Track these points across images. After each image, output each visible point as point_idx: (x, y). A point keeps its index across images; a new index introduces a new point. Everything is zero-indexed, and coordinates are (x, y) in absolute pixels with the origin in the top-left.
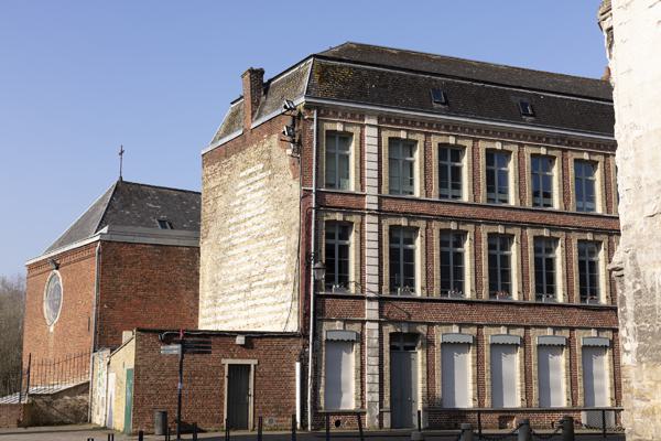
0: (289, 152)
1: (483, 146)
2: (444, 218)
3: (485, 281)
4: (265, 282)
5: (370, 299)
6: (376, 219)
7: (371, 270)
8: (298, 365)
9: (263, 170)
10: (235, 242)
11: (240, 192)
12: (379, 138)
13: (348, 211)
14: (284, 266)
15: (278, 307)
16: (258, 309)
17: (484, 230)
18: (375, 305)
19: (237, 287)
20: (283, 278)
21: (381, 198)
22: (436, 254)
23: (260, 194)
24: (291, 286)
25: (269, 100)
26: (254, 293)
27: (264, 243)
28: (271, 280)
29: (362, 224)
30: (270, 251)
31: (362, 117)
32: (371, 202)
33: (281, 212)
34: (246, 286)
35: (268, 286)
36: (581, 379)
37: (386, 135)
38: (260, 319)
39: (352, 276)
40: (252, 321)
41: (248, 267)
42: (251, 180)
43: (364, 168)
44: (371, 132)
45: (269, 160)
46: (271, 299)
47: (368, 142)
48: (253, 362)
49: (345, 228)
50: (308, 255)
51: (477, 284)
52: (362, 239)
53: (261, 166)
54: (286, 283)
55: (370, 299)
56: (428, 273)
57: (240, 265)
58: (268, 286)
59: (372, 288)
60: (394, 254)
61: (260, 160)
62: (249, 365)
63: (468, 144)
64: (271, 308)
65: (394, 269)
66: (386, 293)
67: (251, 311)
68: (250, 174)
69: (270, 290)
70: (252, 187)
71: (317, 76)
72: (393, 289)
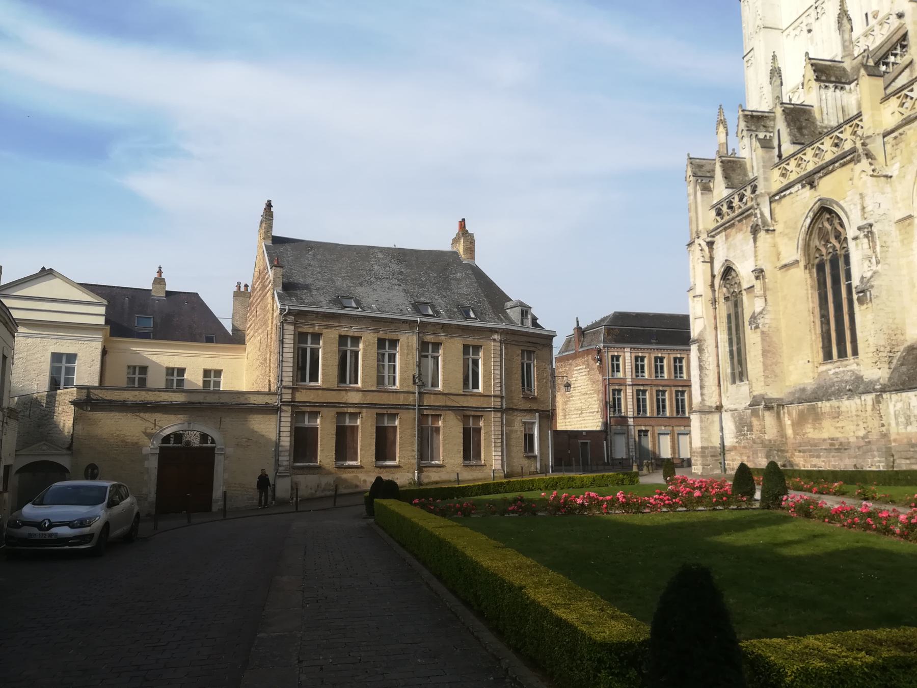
0: (598, 364)
1: (672, 356)
2: (657, 385)
3: (675, 409)
4: (589, 411)
5: (630, 418)
6: (631, 387)
7: (630, 407)
8: (605, 442)
9: (585, 368)
10: (573, 395)
11: (575, 375)
12: (631, 356)
13: (621, 385)
14: (597, 406)
15: (594, 421)
16: (585, 422)
17: (674, 389)
18: (632, 420)
19: (575, 412)
20: (597, 410)
21: (632, 379)
22: (655, 399)
23: (585, 377)
24: (600, 413)
25: (585, 339)
26: (583, 415)
27: (587, 396)
28: (591, 411)
29: (626, 390)
30: (590, 400)
31: (624, 348)
32: (629, 381)
33: (594, 385)
34: (580, 412)
35: (590, 413)
36: (675, 447)
37: (633, 355)
38: (587, 425)
39: (623, 411)
40: (583, 425)
41: (580, 405)
42: (580, 371)
43: (626, 371)
44: (628, 355)
45: (588, 365)
46: (592, 418)
47: (627, 357)
48: (589, 441)
49: (619, 391)
50: (606, 402)
51: (671, 411)
52: (626, 395)
53: (584, 367)
54: (598, 412)
55: (630, 418)
56: (652, 407)
57: (577, 403)
58: (590, 413)
59: (630, 414)
60: (638, 400)
61: (584, 364)
62: (587, 443)
63: (666, 356)
64: (591, 421)
65: (639, 407)
66: (636, 415)
67: (582, 422)
68: (579, 369)
69: (591, 414)
70: (581, 374)
71: (606, 334)
72: (638, 414)
